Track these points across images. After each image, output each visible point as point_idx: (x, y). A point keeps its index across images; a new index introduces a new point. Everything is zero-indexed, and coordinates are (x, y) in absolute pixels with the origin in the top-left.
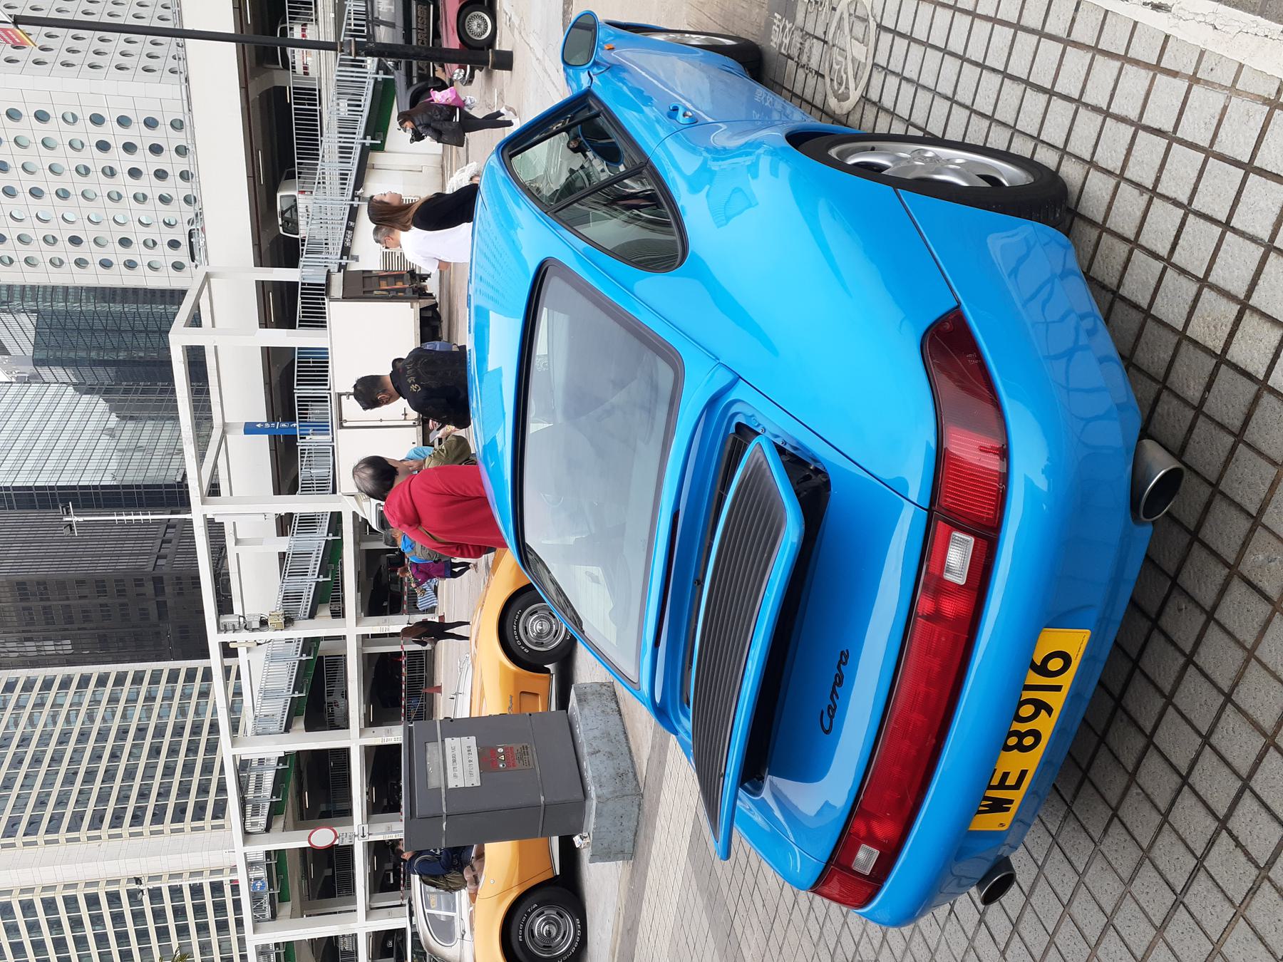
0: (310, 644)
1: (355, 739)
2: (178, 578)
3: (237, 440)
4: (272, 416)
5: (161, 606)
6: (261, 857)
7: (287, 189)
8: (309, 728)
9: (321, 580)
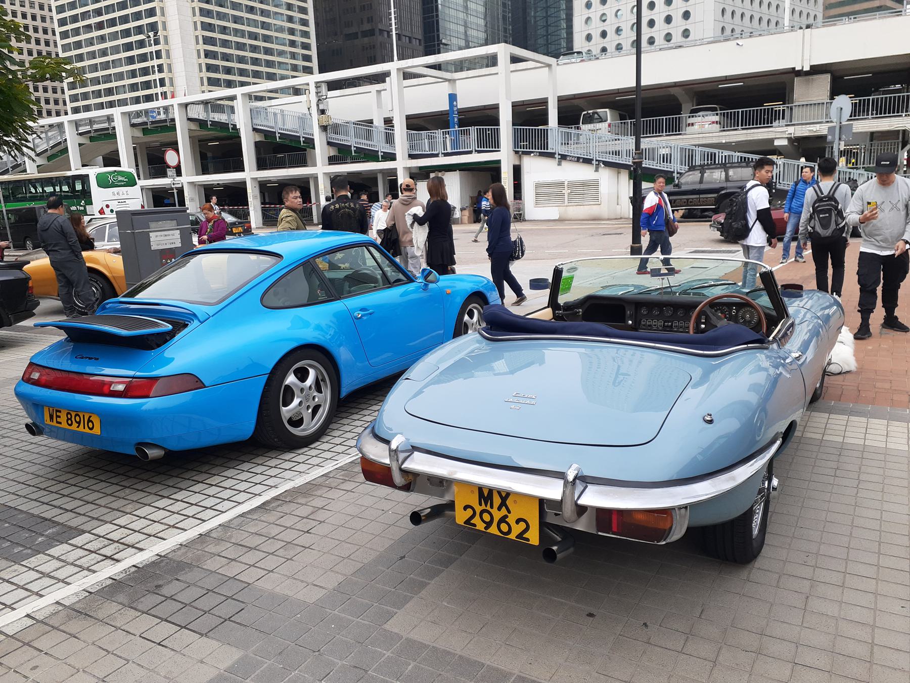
0: (310, 142)
1: (250, 175)
2: (374, 46)
3: (445, 89)
4: (462, 112)
5: (354, 36)
6: (171, 116)
7: (611, 116)
8: (257, 145)
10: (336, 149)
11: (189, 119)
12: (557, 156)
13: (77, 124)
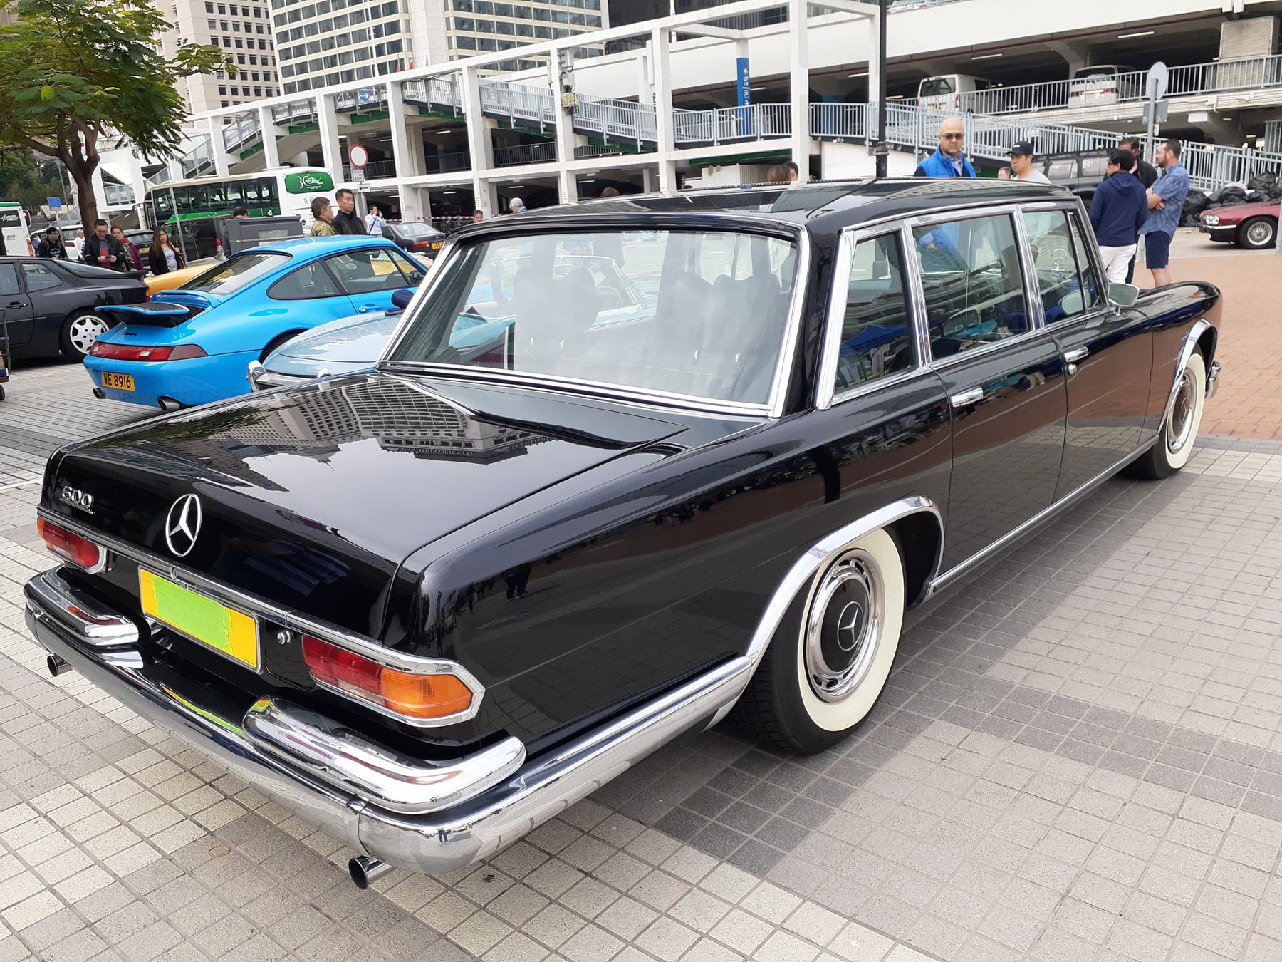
0: (551, 128)
1: (480, 173)
3: (732, 53)
4: (753, 83)
6: (383, 97)
7: (962, 85)
9: (605, 137)
10: (585, 138)
11: (405, 102)
12: (867, 142)
13: (274, 111)
